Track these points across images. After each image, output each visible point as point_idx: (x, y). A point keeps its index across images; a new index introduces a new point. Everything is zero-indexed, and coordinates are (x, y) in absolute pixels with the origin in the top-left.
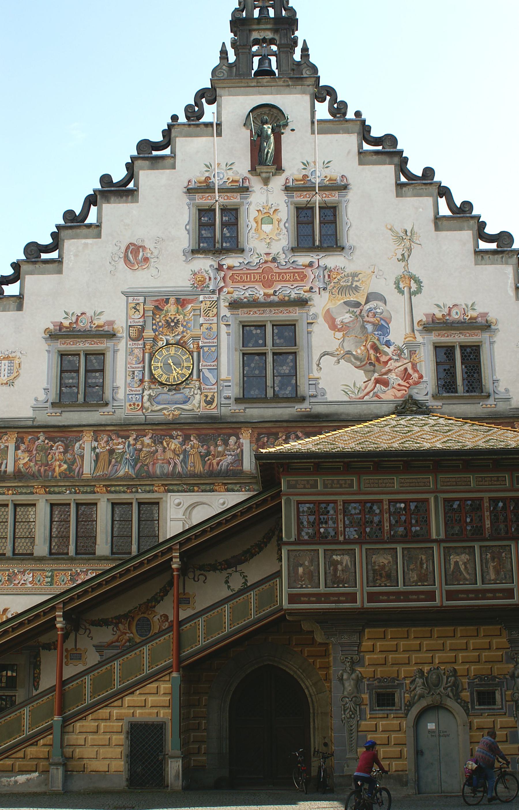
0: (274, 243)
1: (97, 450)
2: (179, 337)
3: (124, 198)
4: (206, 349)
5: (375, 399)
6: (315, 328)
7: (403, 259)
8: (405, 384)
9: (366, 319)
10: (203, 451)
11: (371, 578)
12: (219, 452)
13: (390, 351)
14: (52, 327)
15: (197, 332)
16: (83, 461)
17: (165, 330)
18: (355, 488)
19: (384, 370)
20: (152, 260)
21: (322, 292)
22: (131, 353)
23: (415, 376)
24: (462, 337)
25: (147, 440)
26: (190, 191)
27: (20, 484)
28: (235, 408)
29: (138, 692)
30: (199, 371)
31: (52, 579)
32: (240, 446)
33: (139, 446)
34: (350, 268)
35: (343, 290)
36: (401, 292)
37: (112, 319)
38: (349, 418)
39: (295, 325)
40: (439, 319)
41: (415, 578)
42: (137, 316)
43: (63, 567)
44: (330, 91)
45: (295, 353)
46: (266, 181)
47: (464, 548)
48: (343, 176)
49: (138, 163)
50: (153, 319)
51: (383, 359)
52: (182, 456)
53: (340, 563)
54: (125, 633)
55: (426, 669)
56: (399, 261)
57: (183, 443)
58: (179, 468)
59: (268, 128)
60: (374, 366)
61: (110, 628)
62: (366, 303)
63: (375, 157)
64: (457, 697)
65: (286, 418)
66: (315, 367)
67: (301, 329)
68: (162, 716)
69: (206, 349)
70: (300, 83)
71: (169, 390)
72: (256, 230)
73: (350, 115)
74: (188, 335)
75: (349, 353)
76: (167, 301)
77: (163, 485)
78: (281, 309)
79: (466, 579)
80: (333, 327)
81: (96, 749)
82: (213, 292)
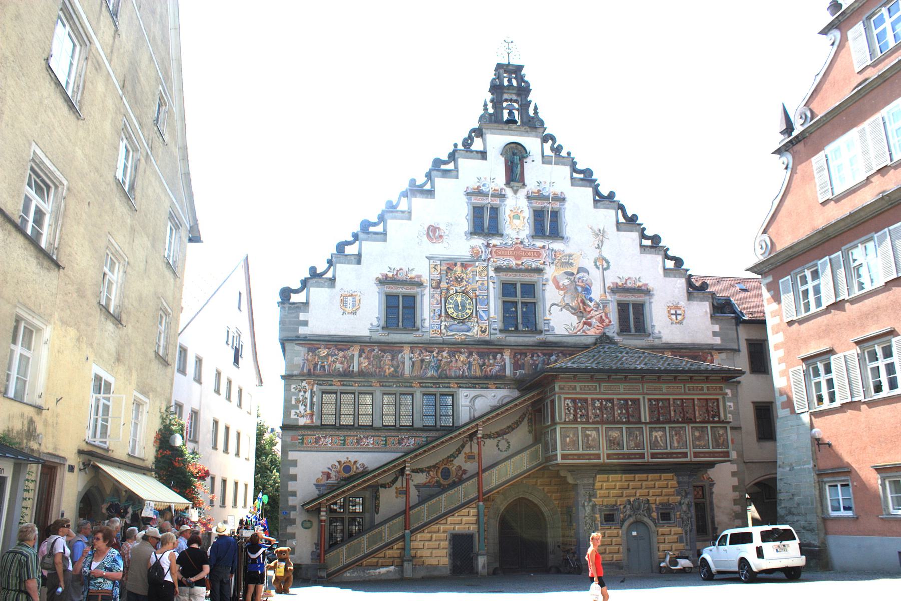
0: (521, 232)
1: (413, 359)
2: (463, 289)
3: (426, 196)
4: (480, 297)
5: (583, 334)
6: (547, 288)
7: (598, 247)
8: (601, 325)
9: (577, 284)
10: (481, 362)
11: (608, 445)
12: (490, 363)
13: (591, 304)
14: (381, 277)
15: (474, 286)
16: (404, 366)
17: (454, 283)
18: (598, 391)
19: (588, 316)
20: (445, 237)
21: (551, 265)
22: (433, 297)
23: (607, 320)
24: (634, 298)
25: (445, 354)
26: (468, 194)
27: (364, 380)
28: (499, 335)
29: (456, 515)
30: (476, 311)
31: (386, 442)
32: (503, 360)
33: (440, 358)
34: (568, 252)
35: (563, 265)
36: (598, 268)
37: (420, 274)
38: (569, 345)
39: (534, 285)
40: (620, 286)
41: (633, 445)
42: (436, 273)
43: (393, 434)
44: (553, 138)
45: (535, 302)
46: (515, 192)
47: (660, 428)
48: (561, 193)
49: (434, 173)
50: (447, 276)
51: (588, 309)
52: (467, 365)
53: (590, 435)
54: (434, 478)
55: (632, 499)
56: (596, 248)
57: (468, 357)
58: (466, 373)
59: (516, 158)
60: (583, 313)
61: (425, 474)
62: (577, 273)
63: (580, 182)
64: (650, 517)
65: (531, 343)
66: (547, 312)
67: (538, 288)
68: (471, 529)
69: (480, 297)
70: (534, 130)
71: (458, 322)
72: (510, 222)
73: (564, 153)
74: (469, 287)
75: (568, 304)
76: (455, 265)
77: (456, 383)
78: (526, 274)
79: (661, 446)
80: (558, 287)
81: (430, 551)
82: (484, 261)
